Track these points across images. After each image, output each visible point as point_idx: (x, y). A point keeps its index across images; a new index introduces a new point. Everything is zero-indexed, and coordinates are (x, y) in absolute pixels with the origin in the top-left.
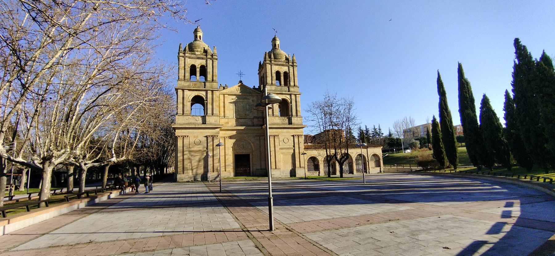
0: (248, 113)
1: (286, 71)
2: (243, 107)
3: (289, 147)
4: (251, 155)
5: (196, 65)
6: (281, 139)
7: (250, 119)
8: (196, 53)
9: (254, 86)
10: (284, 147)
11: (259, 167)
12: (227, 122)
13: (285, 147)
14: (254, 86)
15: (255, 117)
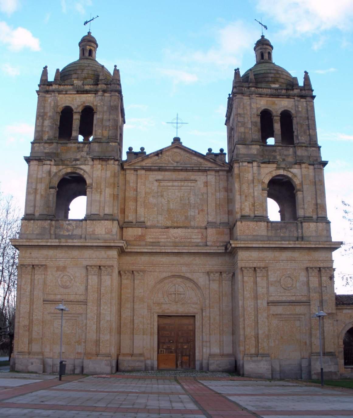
0: (193, 214)
1: (285, 109)
2: (181, 200)
3: (293, 298)
4: (198, 317)
5: (73, 108)
6: (272, 278)
7: (197, 228)
8: (75, 82)
9: (210, 150)
10: (280, 299)
11: (216, 350)
12: (140, 236)
13: (284, 299)
14: (210, 150)
15: (210, 224)
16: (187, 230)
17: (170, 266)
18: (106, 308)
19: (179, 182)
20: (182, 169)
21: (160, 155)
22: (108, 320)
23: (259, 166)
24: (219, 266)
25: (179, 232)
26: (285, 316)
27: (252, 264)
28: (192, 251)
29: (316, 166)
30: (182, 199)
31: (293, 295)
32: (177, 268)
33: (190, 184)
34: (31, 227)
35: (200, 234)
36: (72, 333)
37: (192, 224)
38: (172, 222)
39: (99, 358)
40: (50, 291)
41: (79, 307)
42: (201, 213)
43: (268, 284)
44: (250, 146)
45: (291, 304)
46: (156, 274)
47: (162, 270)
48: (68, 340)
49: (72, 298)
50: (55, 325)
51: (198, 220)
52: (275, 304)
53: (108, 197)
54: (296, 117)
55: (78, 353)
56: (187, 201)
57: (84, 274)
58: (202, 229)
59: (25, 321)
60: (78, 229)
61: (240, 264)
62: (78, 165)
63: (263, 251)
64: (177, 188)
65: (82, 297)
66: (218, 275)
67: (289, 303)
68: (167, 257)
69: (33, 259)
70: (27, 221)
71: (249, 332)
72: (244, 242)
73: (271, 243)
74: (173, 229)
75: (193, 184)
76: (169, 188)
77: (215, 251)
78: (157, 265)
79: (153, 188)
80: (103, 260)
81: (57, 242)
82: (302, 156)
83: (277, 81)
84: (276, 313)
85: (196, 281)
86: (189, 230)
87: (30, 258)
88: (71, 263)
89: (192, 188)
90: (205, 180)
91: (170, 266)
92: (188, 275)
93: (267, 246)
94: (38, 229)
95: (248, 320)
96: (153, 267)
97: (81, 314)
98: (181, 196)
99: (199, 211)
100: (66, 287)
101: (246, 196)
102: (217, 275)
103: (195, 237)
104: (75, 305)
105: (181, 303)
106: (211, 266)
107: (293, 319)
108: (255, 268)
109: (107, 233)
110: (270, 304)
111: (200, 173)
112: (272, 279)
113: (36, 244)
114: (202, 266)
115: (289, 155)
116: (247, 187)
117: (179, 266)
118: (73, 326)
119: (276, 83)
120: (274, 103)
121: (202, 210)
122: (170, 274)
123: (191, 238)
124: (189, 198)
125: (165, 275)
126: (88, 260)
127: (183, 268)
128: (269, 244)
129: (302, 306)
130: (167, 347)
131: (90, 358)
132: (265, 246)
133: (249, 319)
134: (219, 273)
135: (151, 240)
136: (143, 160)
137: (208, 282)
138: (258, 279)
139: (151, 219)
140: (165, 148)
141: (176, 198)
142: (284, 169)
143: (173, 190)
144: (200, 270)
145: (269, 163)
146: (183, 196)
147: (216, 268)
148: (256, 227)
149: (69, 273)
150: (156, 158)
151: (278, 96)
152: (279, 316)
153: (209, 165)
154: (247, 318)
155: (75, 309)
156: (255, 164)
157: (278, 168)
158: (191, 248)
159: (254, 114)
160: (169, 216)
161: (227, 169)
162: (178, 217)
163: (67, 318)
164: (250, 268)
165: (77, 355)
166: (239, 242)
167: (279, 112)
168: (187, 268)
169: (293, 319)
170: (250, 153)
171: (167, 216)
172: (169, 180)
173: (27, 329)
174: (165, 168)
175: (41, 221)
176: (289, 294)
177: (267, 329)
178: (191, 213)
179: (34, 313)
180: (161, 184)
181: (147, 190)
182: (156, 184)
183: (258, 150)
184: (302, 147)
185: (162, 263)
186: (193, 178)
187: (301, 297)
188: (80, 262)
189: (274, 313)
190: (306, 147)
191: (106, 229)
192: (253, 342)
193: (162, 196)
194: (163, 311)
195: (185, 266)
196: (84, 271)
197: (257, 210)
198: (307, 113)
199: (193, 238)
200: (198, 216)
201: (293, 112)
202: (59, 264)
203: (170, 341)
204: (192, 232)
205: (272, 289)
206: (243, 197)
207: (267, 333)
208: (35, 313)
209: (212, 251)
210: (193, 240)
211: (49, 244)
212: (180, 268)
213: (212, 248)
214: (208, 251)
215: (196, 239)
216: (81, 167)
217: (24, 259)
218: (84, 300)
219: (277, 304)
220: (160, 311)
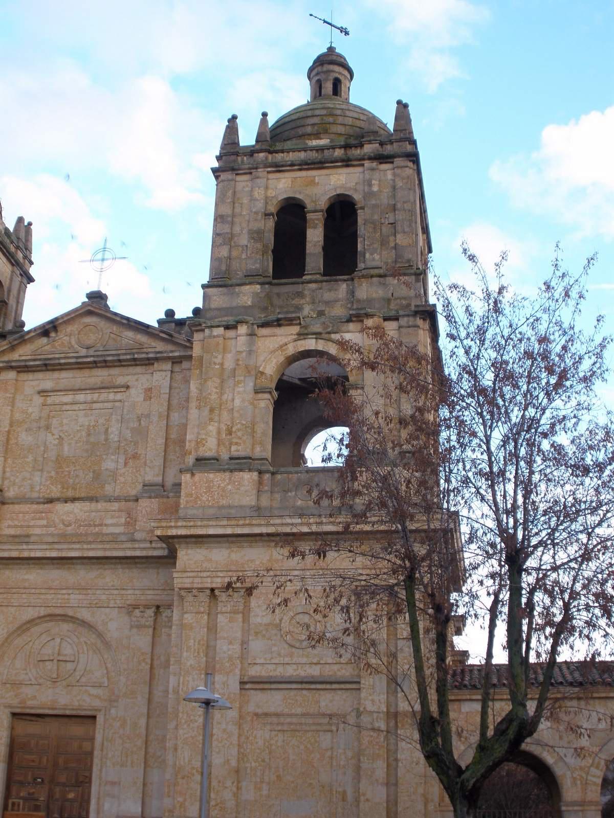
1: (339, 192)
2: (89, 435)
3: (315, 671)
7: (117, 499)
10: (279, 672)
13: (290, 672)
14: (170, 313)
16: (94, 505)
17: (43, 591)
19: (88, 392)
20: (95, 362)
21: (53, 334)
23: (252, 334)
24: (159, 592)
25: (76, 511)
26: (289, 720)
27: (209, 580)
28: (91, 554)
29: (403, 321)
30: (92, 432)
31: (315, 661)
32: (60, 596)
33: (111, 396)
35: (124, 515)
37: (109, 489)
38: (63, 488)
42: (131, 463)
43: (246, 631)
44: (237, 289)
45: (304, 686)
46: (12, 610)
47: (25, 600)
51: (122, 479)
52: (261, 686)
54: (362, 208)
56: (103, 437)
58: (129, 501)
61: (179, 580)
63: (243, 547)
64: (82, 407)
66: (153, 615)
67: (302, 683)
68: (39, 571)
71: (186, 760)
72: (184, 524)
73: (254, 522)
74: (62, 505)
75: (119, 396)
76: (65, 407)
77: (144, 553)
78: (14, 590)
79: (30, 410)
82: (370, 301)
83: (326, 132)
84: (266, 711)
85: (100, 628)
86: (100, 506)
89: (117, 404)
90: (147, 385)
91: (43, 591)
92: (85, 614)
93: (246, 531)
95: (185, 726)
96: (5, 596)
98: (89, 426)
99: (126, 459)
101: (212, 410)
102: (150, 612)
103: (109, 521)
105: (64, 683)
106: (137, 592)
107: (314, 728)
108: (212, 590)
110: (248, 686)
111: (139, 369)
112: (259, 620)
114: (116, 592)
115: (336, 301)
116: (216, 388)
117: (64, 592)
119: (322, 136)
120: (312, 183)
121: (135, 457)
122: (43, 612)
123: (101, 525)
124: (107, 429)
125: (30, 613)
127: (72, 596)
128: (251, 525)
129: (339, 692)
130: (29, 794)
132: (239, 531)
133: (189, 725)
134: (153, 609)
135: (12, 532)
136: (13, 348)
138: (220, 618)
139: (17, 481)
140: (62, 316)
141: (78, 431)
142: (318, 335)
143: (74, 412)
144: (112, 602)
145: (278, 323)
146: (94, 426)
147: (149, 597)
148: (228, 484)
150: (44, 340)
151: (319, 165)
152: (275, 720)
153: (160, 346)
154: (183, 721)
156: (243, 329)
157: (302, 336)
158: (89, 546)
159: (256, 213)
160: (57, 473)
162: (77, 476)
164: (201, 590)
166: (173, 524)
167: (323, 203)
168: (81, 597)
169: (314, 728)
170: (234, 304)
171: (53, 473)
172: (65, 390)
174: (57, 361)
176: (304, 660)
177: (234, 751)
178: (109, 464)
180: (49, 400)
181: (18, 416)
182: (38, 400)
183: (255, 295)
184: (372, 276)
185: (27, 585)
186: (121, 380)
187: (336, 667)
189: (260, 711)
190: (380, 276)
192: (195, 786)
193: (48, 428)
194: (20, 703)
197: (236, 444)
198: (394, 196)
199: (106, 525)
200: (123, 471)
201: (357, 197)
203: (35, 779)
204: (107, 511)
205: (256, 645)
206: (206, 412)
207: (234, 763)
209: (138, 553)
210: (106, 530)
212: (66, 597)
213: (137, 546)
214: (129, 553)
215: (112, 525)
219: (266, 686)
220: (15, 702)
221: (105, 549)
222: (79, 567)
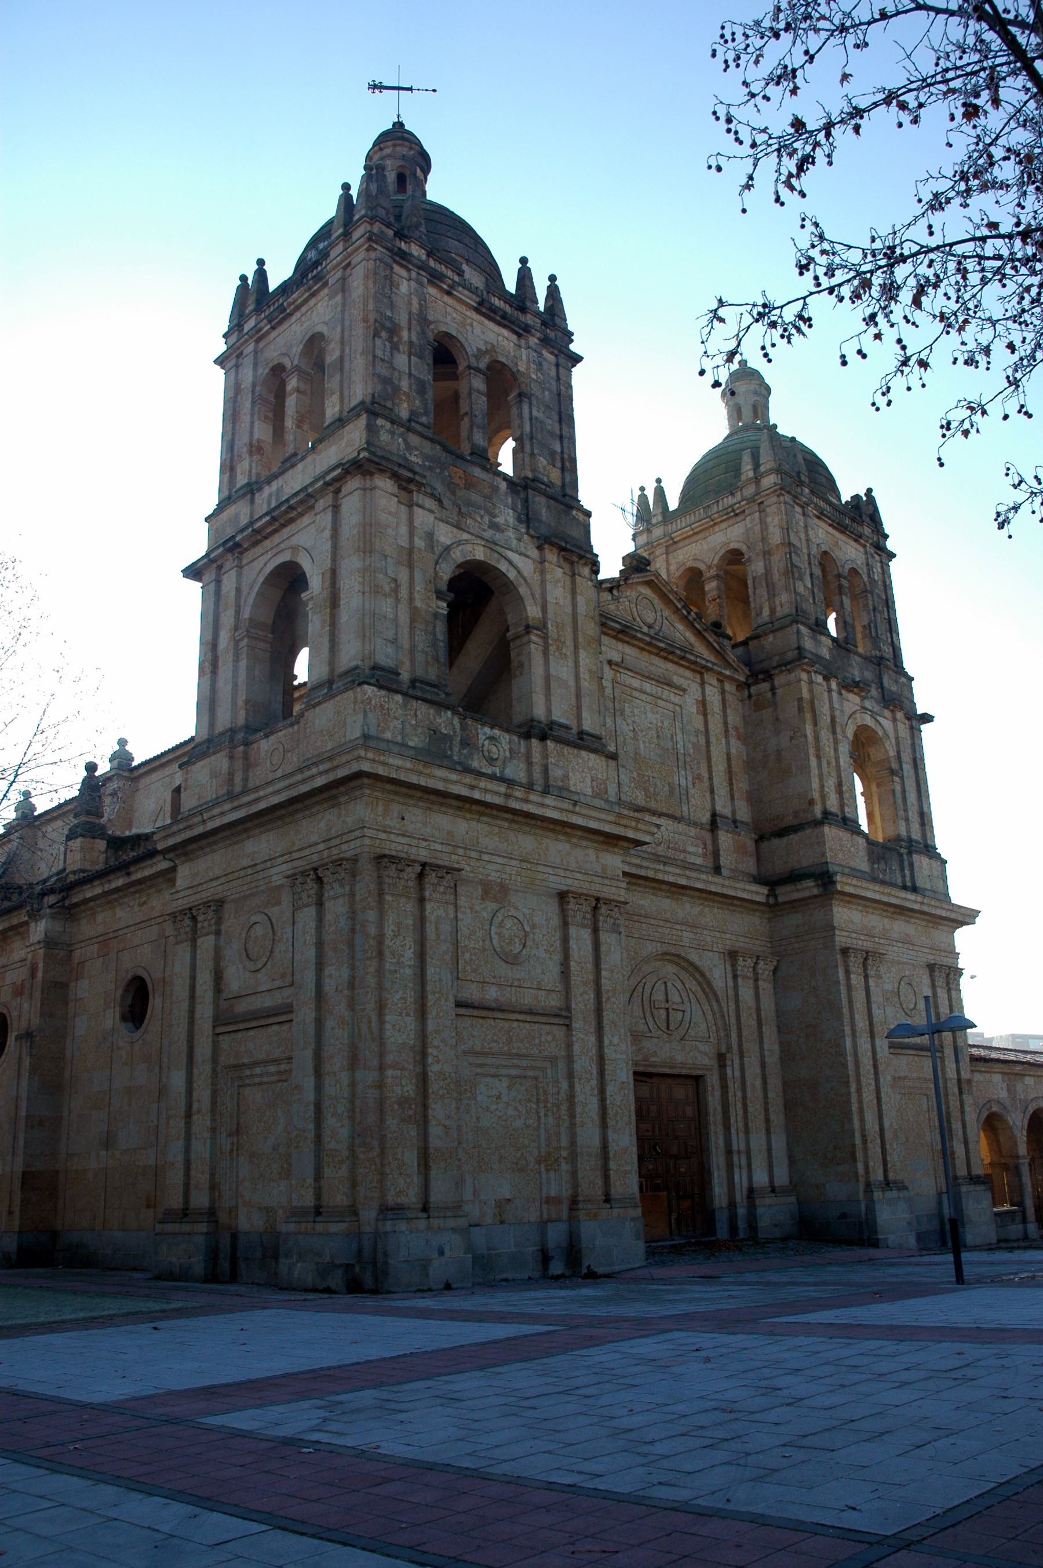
18: (615, 1040)
21: (615, 592)
22: (623, 1083)
32: (674, 932)
34: (395, 718)
36: (528, 1126)
39: (615, 1211)
40: (468, 968)
41: (548, 1033)
47: (644, 933)
48: (519, 1154)
49: (528, 999)
50: (479, 1098)
53: (587, 678)
55: (548, 1200)
57: (556, 921)
59: (404, 1083)
60: (515, 762)
62: (511, 550)
65: (553, 999)
69: (414, 842)
70: (383, 692)
78: (636, 918)
80: (596, 879)
81: (497, 793)
87: (404, 835)
88: (518, 874)
92: (694, 957)
94: (420, 730)
97: (553, 1060)
100: (512, 960)
103: (691, 849)
104: (537, 1026)
109: (596, 795)
113: (440, 786)
117: (678, 927)
118: (530, 1101)
126: (561, 872)
131: (596, 1215)
137: (730, 983)
143: (643, 704)
147: (742, 945)
149: (517, 909)
155: (537, 1041)
160: (639, 774)
161: (742, 679)
163: (513, 1072)
165: (545, 1206)
173: (411, 1113)
174: (634, 633)
175: (427, 705)
179: (430, 1050)
188: (541, 876)
191: (593, 781)
195: (689, 929)
196: (553, 906)
199: (689, 853)
202: (487, 872)
208: (435, 1052)
211: (477, 795)
216: (510, 554)
217: (384, 836)
218: (561, 1009)
221: (723, 886)
222: (685, 898)
